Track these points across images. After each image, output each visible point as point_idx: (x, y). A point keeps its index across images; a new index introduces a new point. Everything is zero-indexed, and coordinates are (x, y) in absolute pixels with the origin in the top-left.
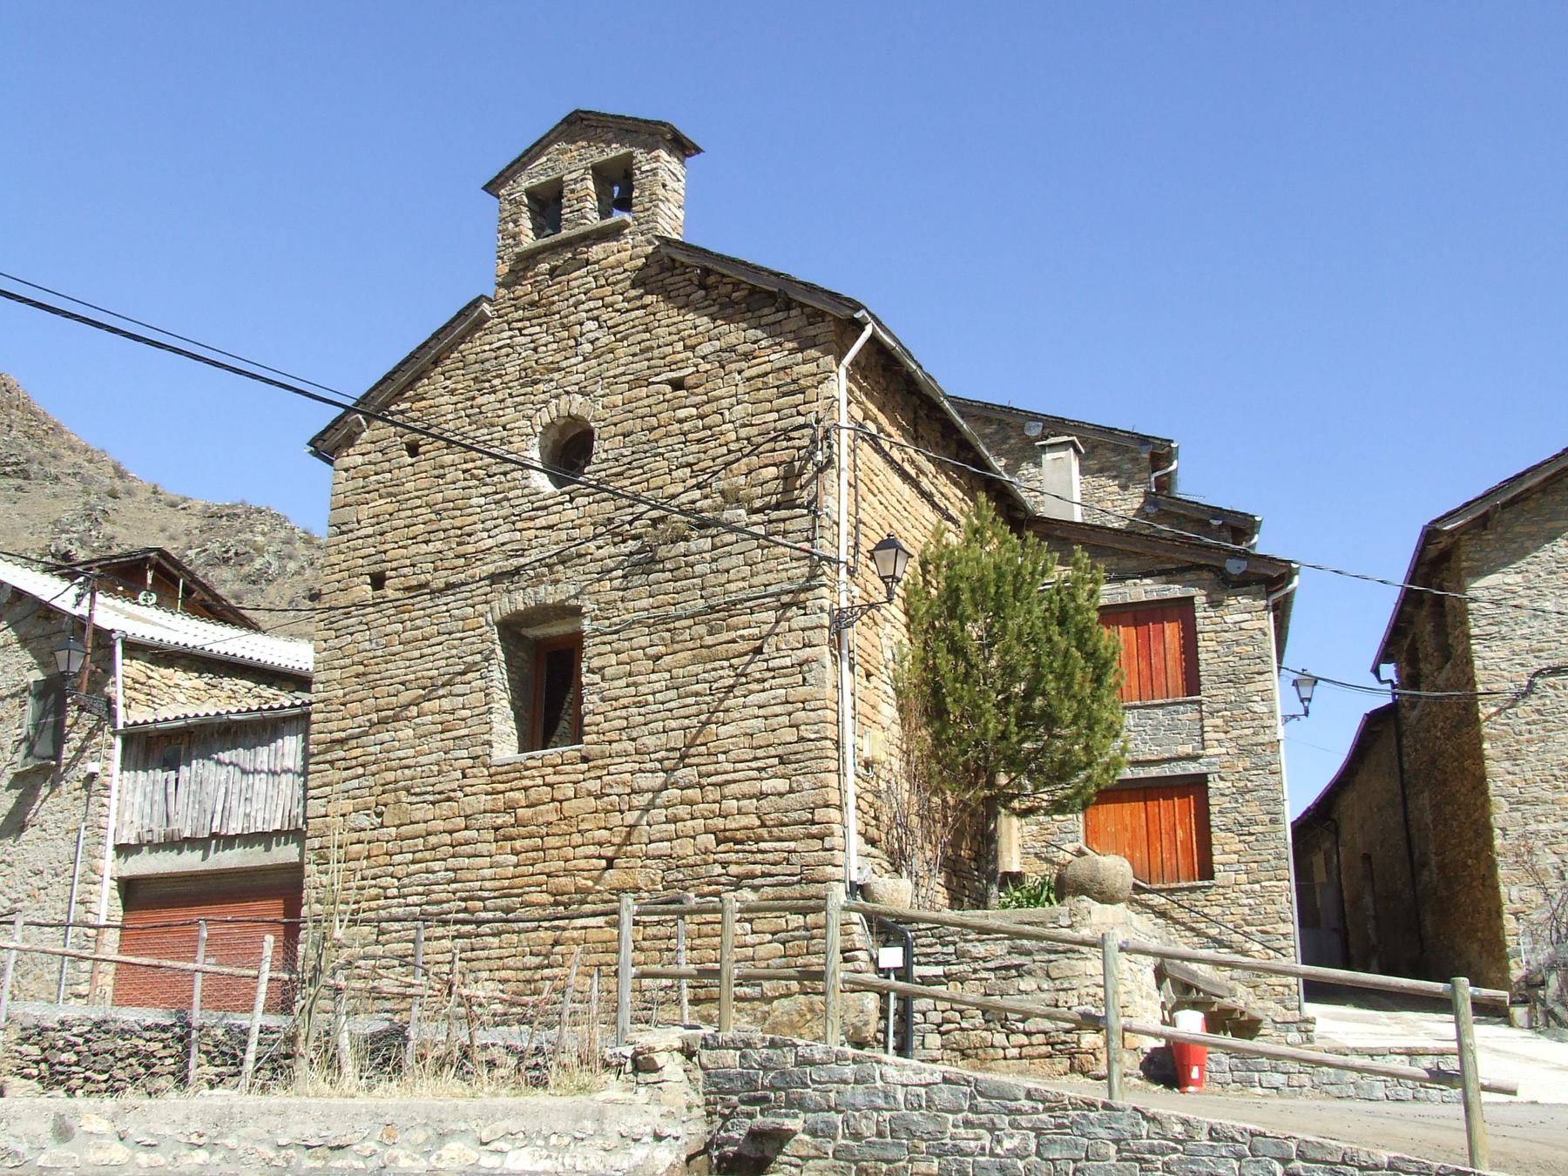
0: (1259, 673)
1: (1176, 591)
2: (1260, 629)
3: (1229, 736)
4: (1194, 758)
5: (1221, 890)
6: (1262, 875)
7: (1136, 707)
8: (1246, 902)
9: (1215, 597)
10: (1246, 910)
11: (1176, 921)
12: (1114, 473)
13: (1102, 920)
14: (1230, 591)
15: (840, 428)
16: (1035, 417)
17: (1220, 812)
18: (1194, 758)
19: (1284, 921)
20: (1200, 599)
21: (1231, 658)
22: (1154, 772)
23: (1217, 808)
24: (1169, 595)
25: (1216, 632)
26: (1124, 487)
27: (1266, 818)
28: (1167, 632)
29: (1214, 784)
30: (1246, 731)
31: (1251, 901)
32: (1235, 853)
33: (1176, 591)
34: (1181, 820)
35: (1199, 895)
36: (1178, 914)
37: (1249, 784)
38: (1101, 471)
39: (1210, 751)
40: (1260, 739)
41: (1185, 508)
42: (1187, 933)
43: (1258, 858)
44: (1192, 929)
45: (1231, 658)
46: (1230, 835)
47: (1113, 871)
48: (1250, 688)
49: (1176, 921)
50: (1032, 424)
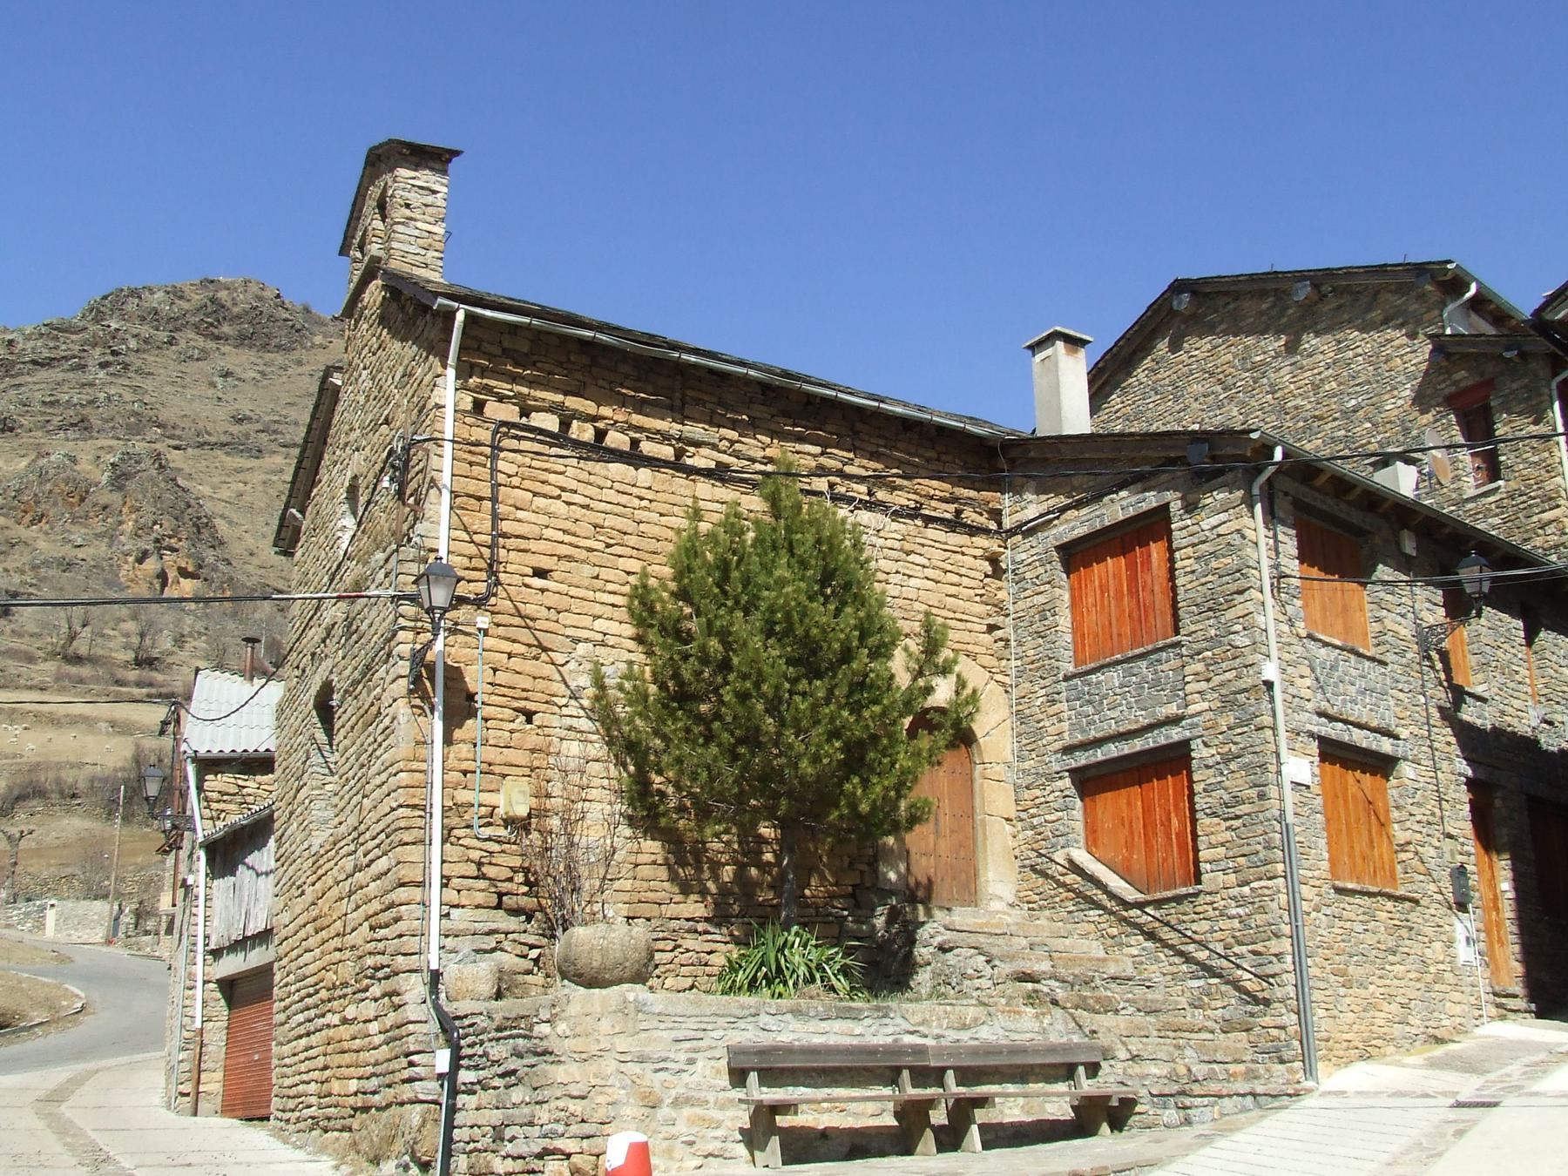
0: (1240, 592)
1: (1151, 500)
2: (1238, 531)
3: (1212, 684)
4: (1175, 721)
5: (1209, 898)
6: (1250, 874)
7: (1118, 663)
8: (1233, 912)
9: (1191, 498)
10: (1236, 923)
11: (1165, 944)
12: (1400, 321)
13: (587, 1010)
14: (1206, 487)
15: (453, 442)
16: (1300, 276)
17: (1205, 790)
18: (1175, 721)
19: (1278, 937)
20: (1176, 507)
21: (1210, 578)
22: (1138, 745)
23: (1202, 785)
24: (1145, 507)
25: (1194, 545)
26: (1412, 336)
27: (1253, 793)
28: (1155, 555)
29: (1199, 752)
30: (1229, 675)
31: (1240, 911)
32: (1222, 845)
33: (1151, 500)
34: (1176, 805)
35: (1186, 907)
36: (1165, 933)
37: (1234, 748)
38: (1386, 322)
39: (1192, 709)
40: (1242, 684)
41: (1474, 345)
42: (1177, 960)
43: (1246, 850)
44: (1181, 954)
45: (1210, 578)
46: (1216, 820)
47: (586, 947)
48: (1230, 614)
49: (1165, 944)
50: (1299, 285)
